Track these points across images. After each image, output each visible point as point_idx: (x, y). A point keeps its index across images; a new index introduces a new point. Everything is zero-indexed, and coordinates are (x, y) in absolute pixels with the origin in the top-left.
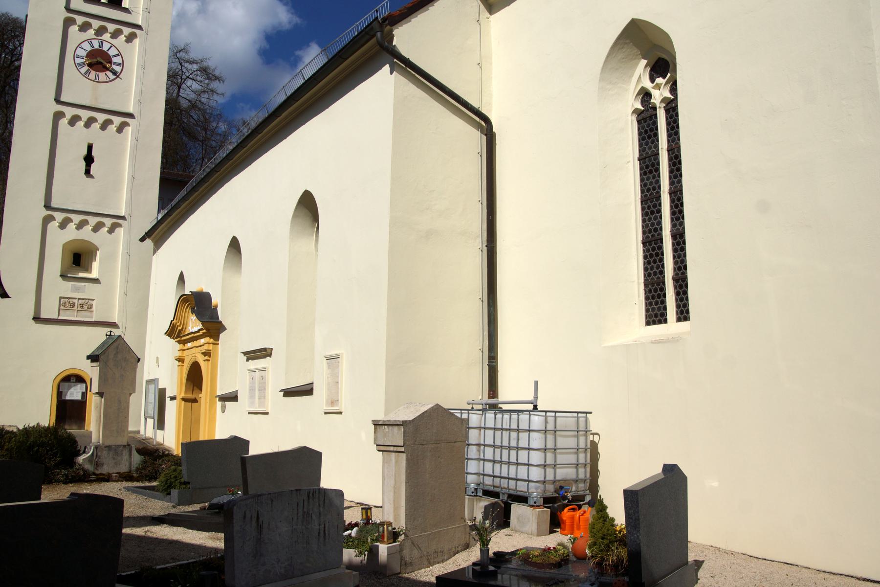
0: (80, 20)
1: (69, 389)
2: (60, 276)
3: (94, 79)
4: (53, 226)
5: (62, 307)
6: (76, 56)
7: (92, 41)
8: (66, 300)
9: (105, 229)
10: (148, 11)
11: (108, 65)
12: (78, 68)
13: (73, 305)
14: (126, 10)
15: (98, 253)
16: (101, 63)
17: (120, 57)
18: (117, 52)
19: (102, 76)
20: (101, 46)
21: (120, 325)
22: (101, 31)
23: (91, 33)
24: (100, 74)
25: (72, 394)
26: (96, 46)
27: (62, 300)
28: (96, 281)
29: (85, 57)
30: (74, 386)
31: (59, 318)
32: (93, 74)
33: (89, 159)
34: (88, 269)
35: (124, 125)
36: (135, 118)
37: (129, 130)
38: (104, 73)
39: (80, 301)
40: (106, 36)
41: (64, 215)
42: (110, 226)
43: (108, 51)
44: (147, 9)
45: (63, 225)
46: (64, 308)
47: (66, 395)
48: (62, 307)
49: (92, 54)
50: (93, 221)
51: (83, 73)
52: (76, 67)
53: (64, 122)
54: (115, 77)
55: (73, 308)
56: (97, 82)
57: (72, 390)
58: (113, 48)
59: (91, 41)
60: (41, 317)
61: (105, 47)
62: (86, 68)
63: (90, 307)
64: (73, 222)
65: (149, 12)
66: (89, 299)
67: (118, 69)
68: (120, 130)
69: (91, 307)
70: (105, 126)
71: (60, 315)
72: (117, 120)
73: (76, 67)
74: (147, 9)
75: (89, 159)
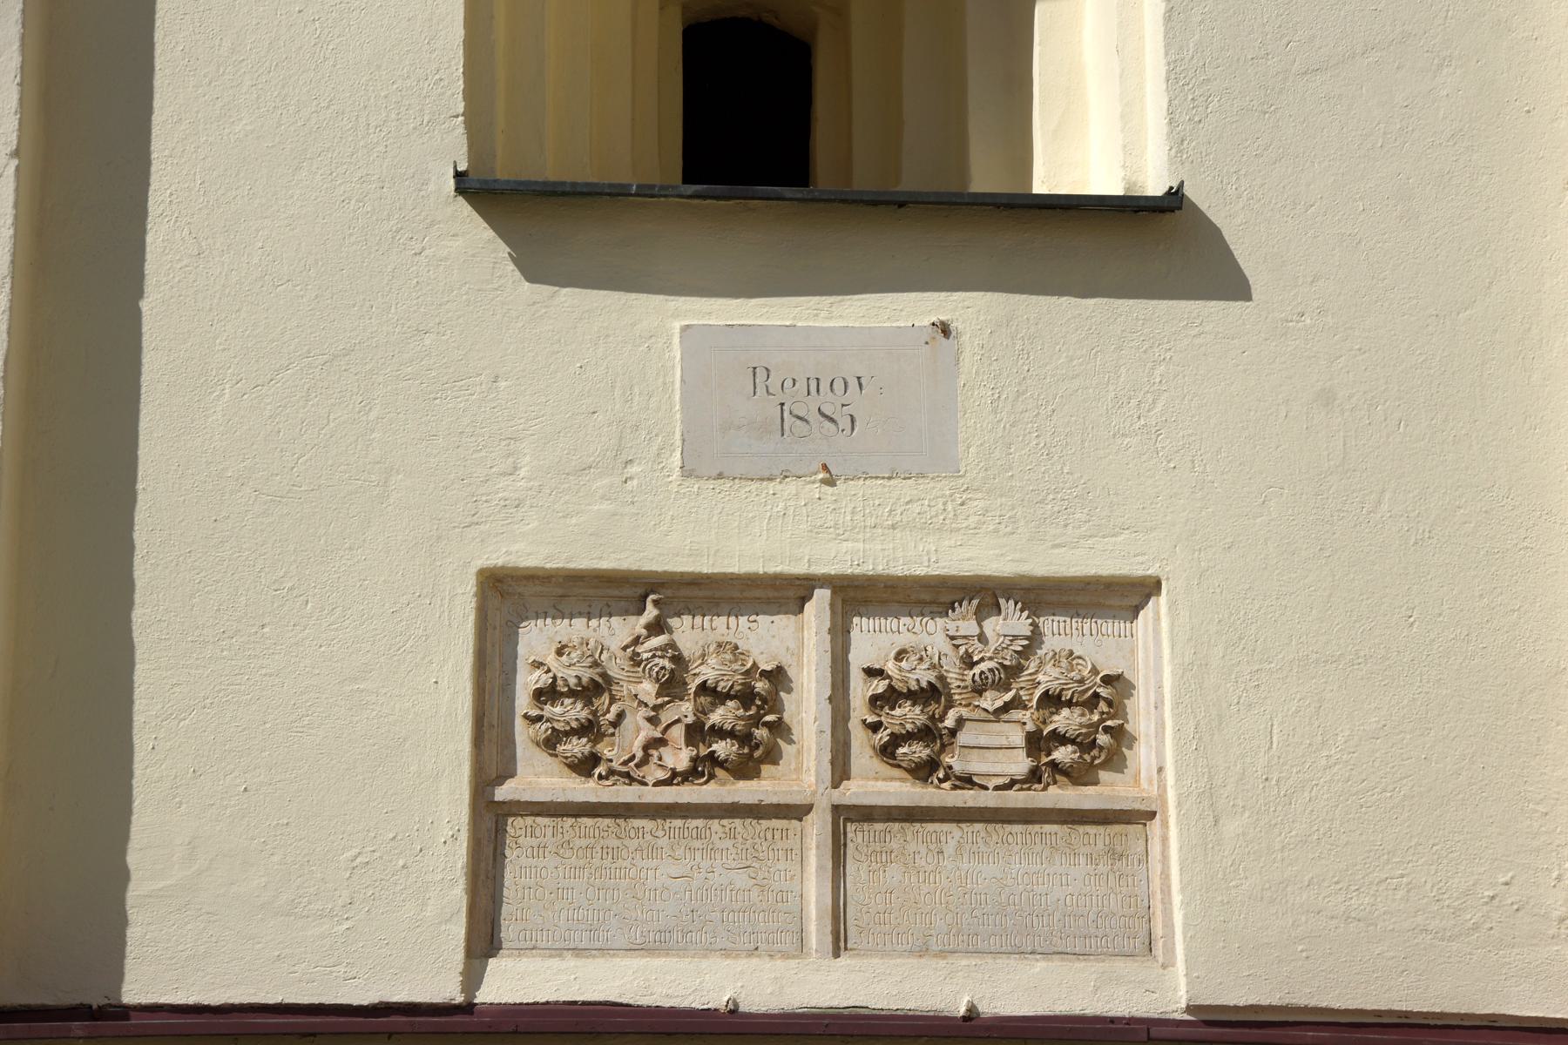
8: (616, 632)
31: (486, 995)
55: (745, 769)
71: (509, 931)
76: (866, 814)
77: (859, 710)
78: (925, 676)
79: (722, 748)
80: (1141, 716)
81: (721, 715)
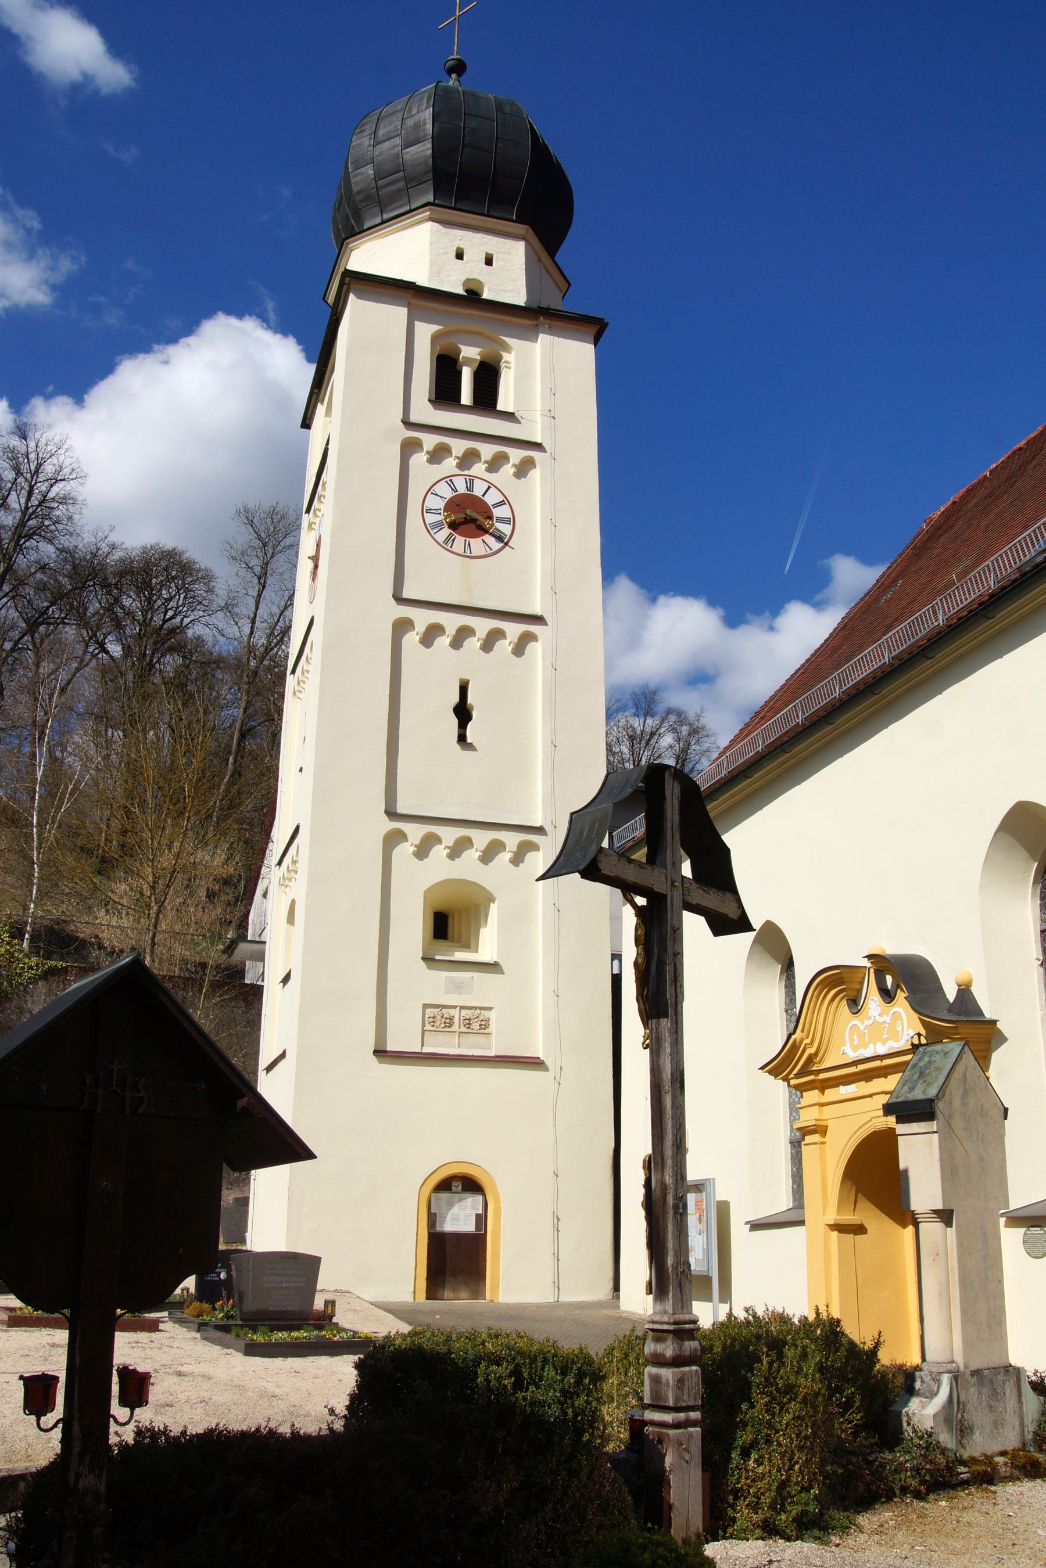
0: (430, 441)
1: (449, 1209)
2: (422, 958)
3: (461, 552)
4: (404, 851)
5: (428, 1027)
6: (425, 511)
7: (454, 479)
8: (436, 1010)
9: (506, 856)
10: (552, 416)
11: (487, 523)
12: (432, 532)
13: (449, 1022)
14: (509, 416)
15: (494, 908)
16: (473, 521)
17: (507, 506)
18: (501, 498)
19: (477, 545)
20: (470, 488)
21: (549, 1062)
22: (469, 458)
23: (450, 464)
24: (473, 541)
25: (456, 1219)
26: (462, 489)
27: (429, 1012)
28: (493, 967)
29: (442, 511)
30: (461, 1200)
31: (423, 1051)
32: (460, 541)
33: (463, 713)
34: (469, 943)
35: (526, 639)
36: (546, 624)
37: (536, 649)
38: (479, 539)
39: (464, 1012)
40: (479, 469)
41: (424, 829)
42: (515, 850)
43: (483, 496)
44: (550, 411)
45: (422, 852)
46: (433, 1029)
47: (443, 1222)
48: (428, 1027)
49: (456, 504)
50: (482, 838)
51: (441, 541)
52: (428, 531)
53: (411, 640)
54: (502, 545)
55: (449, 1027)
56: (468, 557)
57: (455, 1210)
58: (493, 489)
59: (451, 480)
60: (389, 1049)
61: (478, 490)
62: (446, 531)
63: (485, 1025)
64: (441, 844)
65: (554, 418)
66: (481, 1008)
67: (505, 529)
68: (519, 650)
69: (487, 1026)
70: (488, 644)
72: (513, 630)
73: (428, 531)
74: (550, 411)
75: (463, 713)
76: (462, 1033)
77: (462, 1021)
78: (469, 1017)
79: (448, 1025)
80: (491, 1022)
81: (447, 1021)
